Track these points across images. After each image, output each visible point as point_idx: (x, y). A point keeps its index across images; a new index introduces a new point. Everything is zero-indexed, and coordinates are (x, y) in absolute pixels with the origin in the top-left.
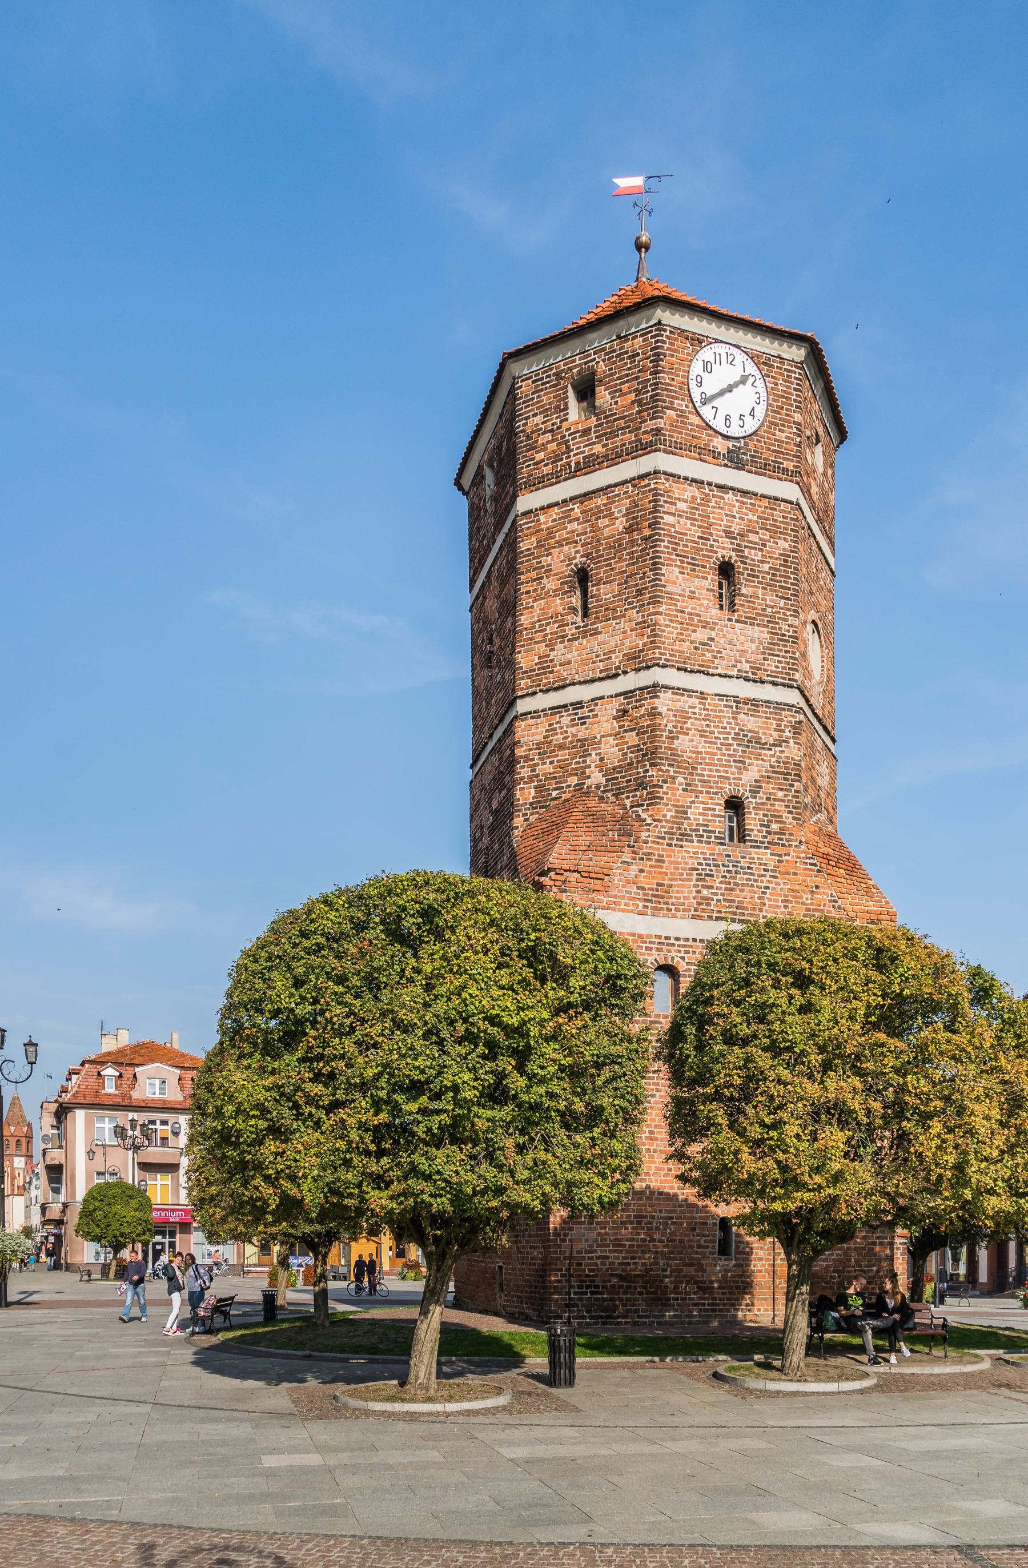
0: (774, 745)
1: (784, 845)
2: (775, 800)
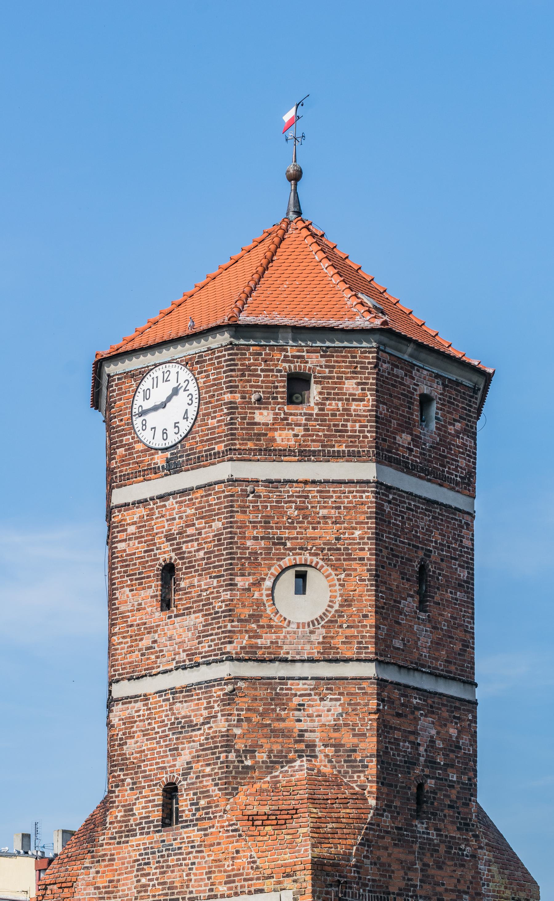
0: (203, 724)
1: (210, 818)
2: (203, 776)
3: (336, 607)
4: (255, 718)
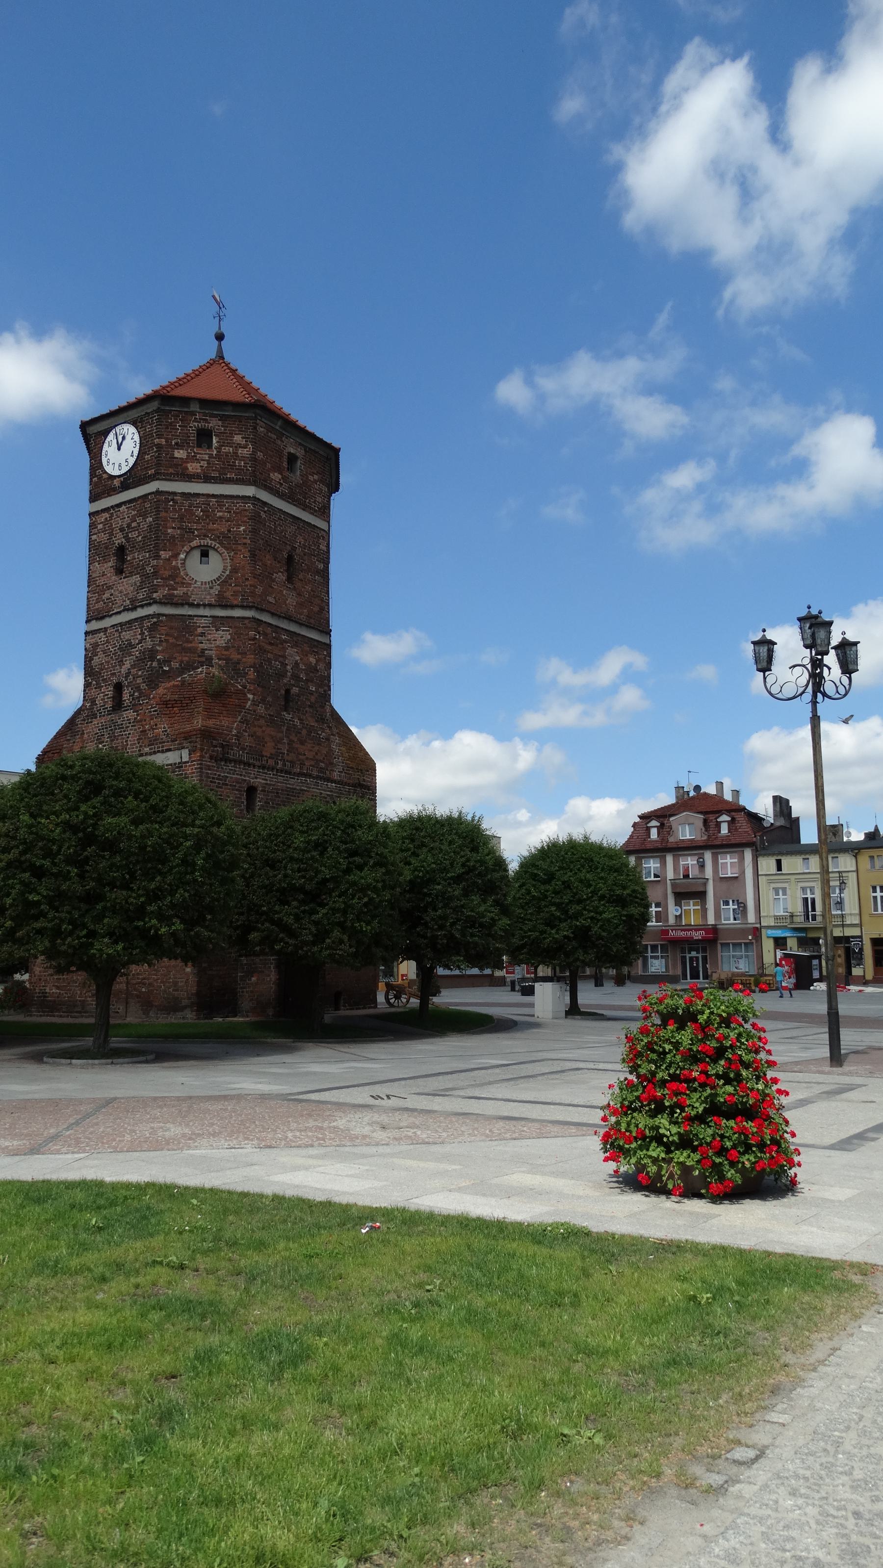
3: (228, 572)
4: (172, 640)
